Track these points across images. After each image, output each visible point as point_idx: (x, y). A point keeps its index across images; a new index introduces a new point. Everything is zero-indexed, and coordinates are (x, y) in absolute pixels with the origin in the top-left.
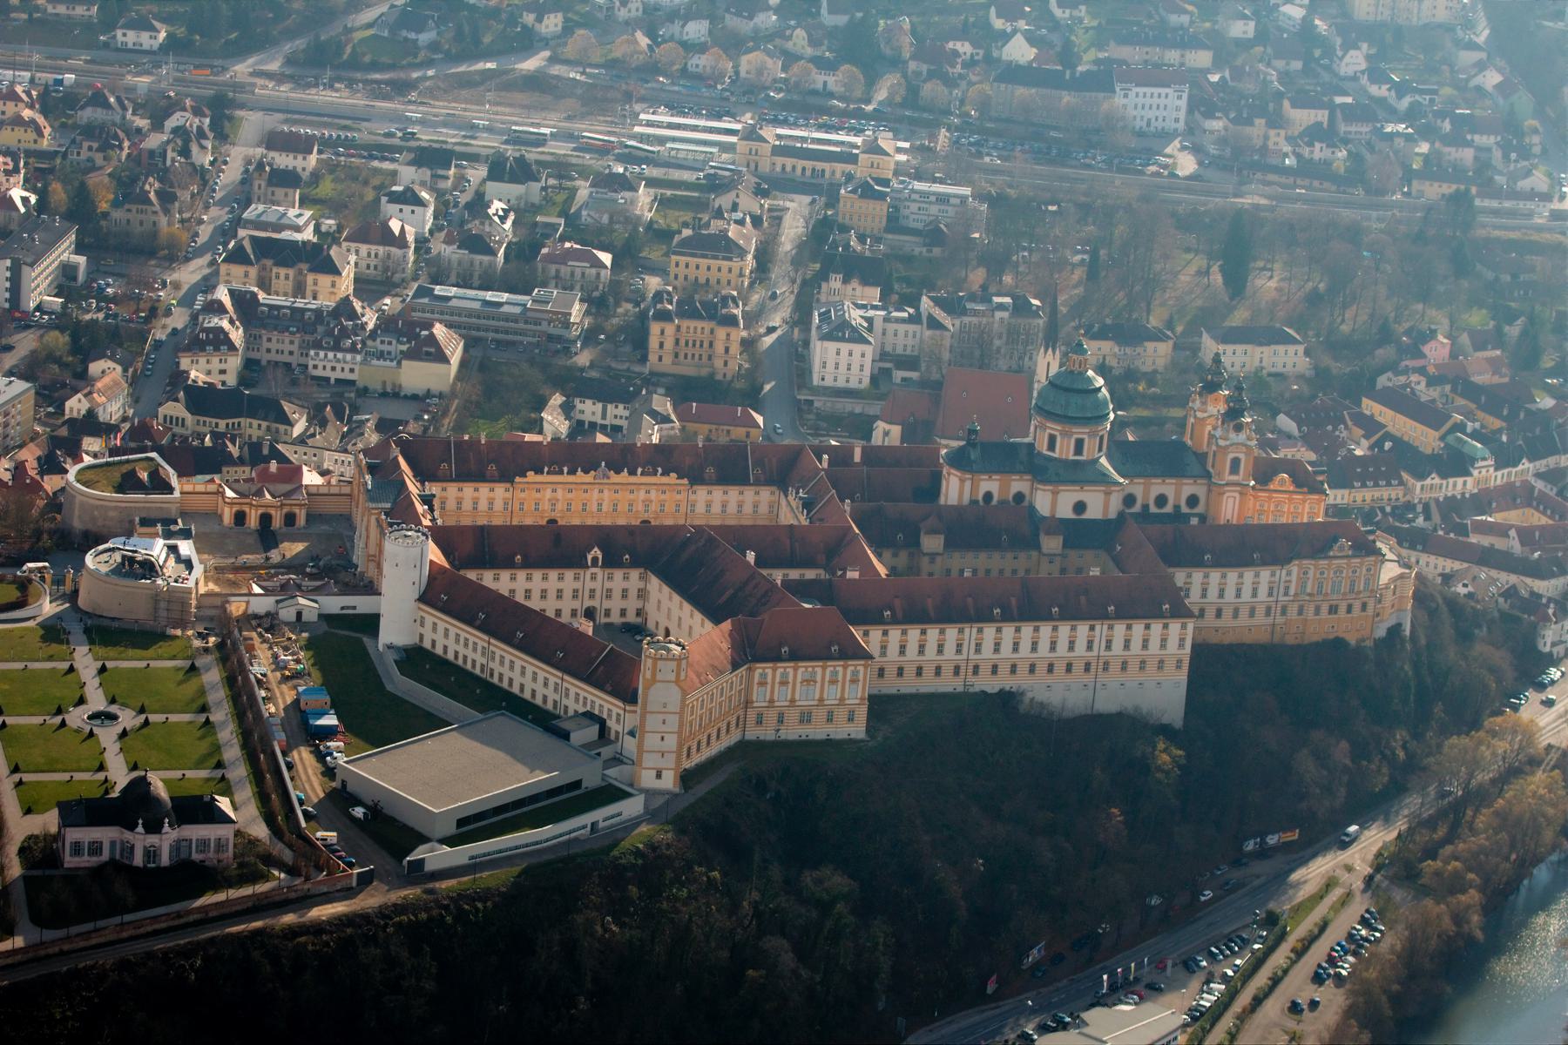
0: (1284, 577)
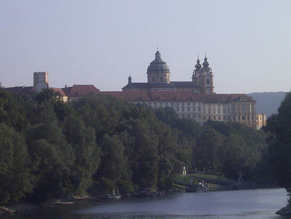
0: (227, 108)
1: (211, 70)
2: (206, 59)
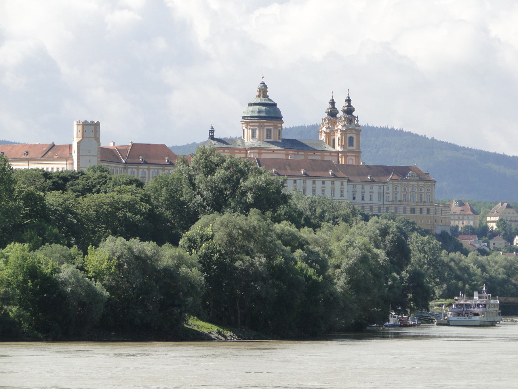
0: (385, 192)
1: (357, 121)
2: (349, 100)
